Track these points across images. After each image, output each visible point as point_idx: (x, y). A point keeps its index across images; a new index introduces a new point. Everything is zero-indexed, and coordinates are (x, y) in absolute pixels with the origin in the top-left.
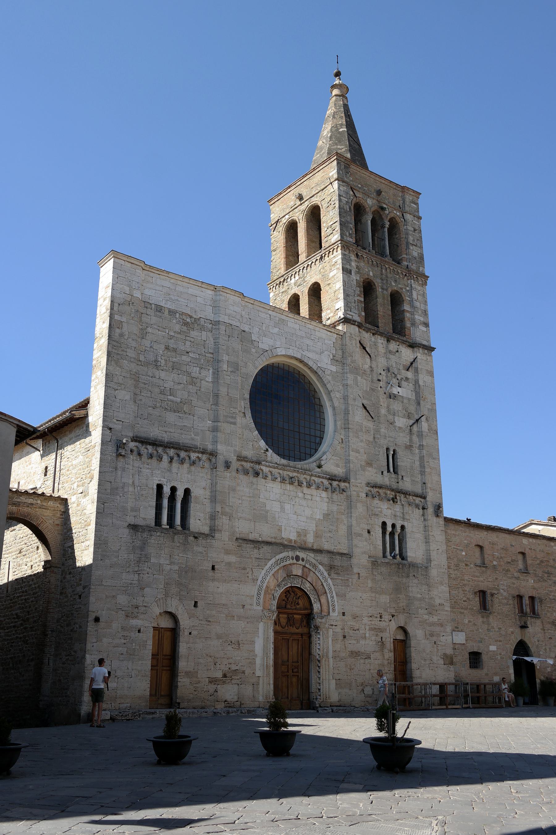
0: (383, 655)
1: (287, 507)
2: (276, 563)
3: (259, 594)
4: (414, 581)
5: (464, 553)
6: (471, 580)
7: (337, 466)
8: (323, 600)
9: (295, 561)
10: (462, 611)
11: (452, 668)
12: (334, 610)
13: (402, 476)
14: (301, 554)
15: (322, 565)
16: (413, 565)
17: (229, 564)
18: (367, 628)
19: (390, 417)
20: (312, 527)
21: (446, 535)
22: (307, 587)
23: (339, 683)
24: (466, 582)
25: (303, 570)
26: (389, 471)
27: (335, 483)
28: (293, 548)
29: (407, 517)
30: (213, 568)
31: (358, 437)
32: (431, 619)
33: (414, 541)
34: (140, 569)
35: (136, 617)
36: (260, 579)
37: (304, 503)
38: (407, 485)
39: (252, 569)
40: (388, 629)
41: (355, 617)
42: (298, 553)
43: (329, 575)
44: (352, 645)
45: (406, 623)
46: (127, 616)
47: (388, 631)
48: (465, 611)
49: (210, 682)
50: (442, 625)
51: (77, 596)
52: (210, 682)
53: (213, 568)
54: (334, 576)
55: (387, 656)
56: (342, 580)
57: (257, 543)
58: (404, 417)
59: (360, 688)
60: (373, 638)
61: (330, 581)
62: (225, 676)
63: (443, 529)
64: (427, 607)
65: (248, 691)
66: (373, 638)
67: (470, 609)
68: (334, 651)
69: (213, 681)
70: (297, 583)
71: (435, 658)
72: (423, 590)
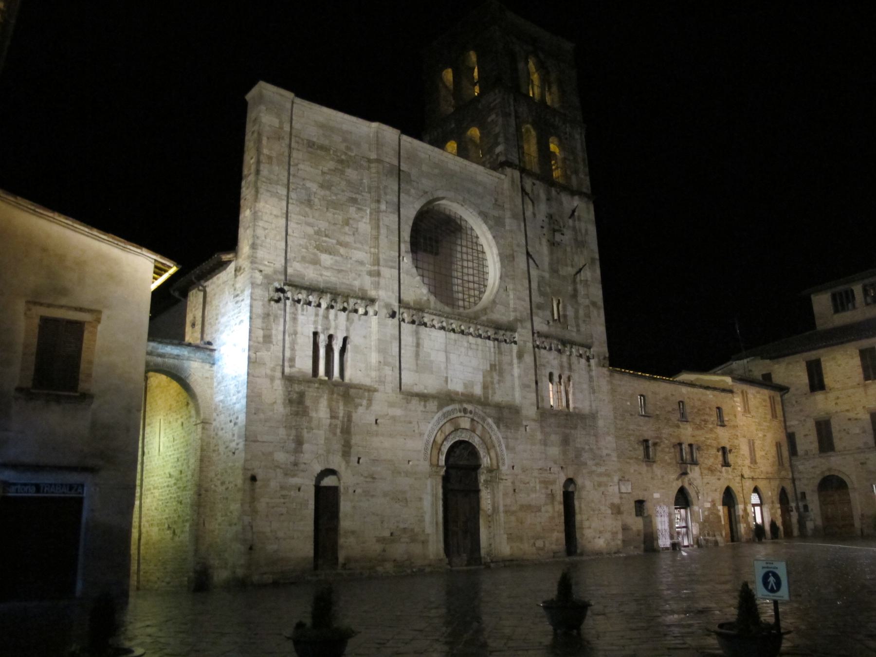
3: (426, 449)
5: (629, 403)
8: (493, 454)
9: (462, 414)
10: (628, 460)
11: (619, 517)
12: (504, 464)
14: (469, 407)
15: (490, 417)
17: (394, 419)
18: (537, 481)
20: (479, 378)
22: (476, 441)
23: (511, 538)
24: (630, 432)
28: (461, 402)
34: (298, 423)
35: (294, 476)
36: (427, 433)
39: (418, 422)
41: (524, 470)
42: (465, 406)
44: (523, 498)
46: (286, 475)
47: (558, 483)
51: (231, 454)
59: (532, 541)
60: (543, 491)
62: (392, 534)
65: (417, 549)
68: (505, 506)
69: (381, 540)
70: (464, 436)
71: (603, 508)
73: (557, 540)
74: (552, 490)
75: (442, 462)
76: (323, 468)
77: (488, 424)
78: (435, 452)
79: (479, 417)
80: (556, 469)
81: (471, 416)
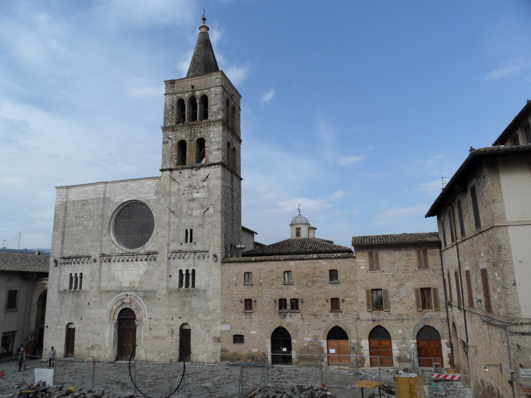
0: (173, 338)
1: (125, 272)
2: (116, 298)
3: (108, 313)
4: (196, 299)
6: (239, 294)
7: (154, 246)
9: (125, 297)
10: (230, 312)
12: (145, 317)
13: (195, 243)
14: (129, 293)
15: (140, 297)
16: (198, 291)
17: (95, 302)
18: (164, 324)
19: (190, 212)
20: (138, 279)
21: (221, 270)
22: (133, 308)
24: (234, 295)
25: (130, 300)
27: (150, 256)
29: (196, 264)
30: (89, 303)
31: (165, 229)
32: (206, 318)
33: (200, 277)
35: (59, 325)
37: (134, 268)
38: (198, 247)
40: (176, 325)
41: (157, 320)
44: (154, 333)
45: (188, 321)
47: (176, 326)
48: (232, 312)
49: (87, 349)
50: (214, 321)
52: (87, 349)
53: (89, 303)
54: (146, 301)
55: (175, 338)
56: (150, 303)
57: (108, 292)
58: (200, 209)
59: (158, 353)
60: (167, 330)
61: (144, 304)
62: (92, 347)
63: (220, 267)
65: (102, 353)
66: (167, 330)
67: (236, 311)
68: (145, 336)
69: (88, 349)
72: (202, 303)
73: (174, 354)
74: (172, 329)
75: (116, 318)
76: (69, 322)
77: (138, 300)
78: (113, 314)
79: (133, 297)
80: (176, 319)
81: (130, 297)
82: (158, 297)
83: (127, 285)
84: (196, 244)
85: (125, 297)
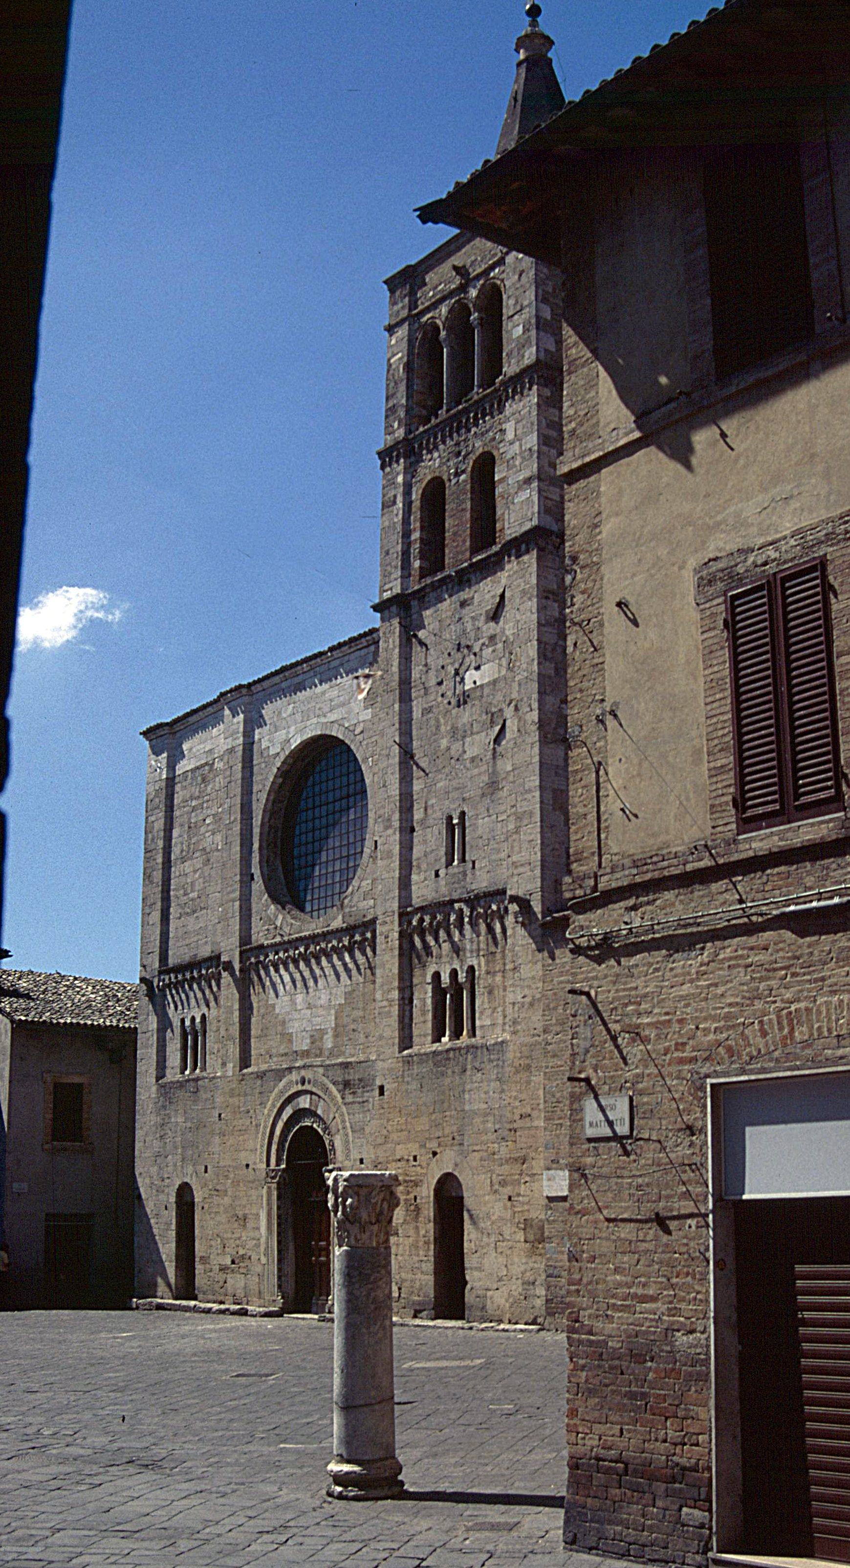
26: (449, 863)
43: (343, 1098)
64: (497, 1127)
82: (378, 1083)
83: (304, 1045)
84: (477, 866)
85: (300, 1087)
